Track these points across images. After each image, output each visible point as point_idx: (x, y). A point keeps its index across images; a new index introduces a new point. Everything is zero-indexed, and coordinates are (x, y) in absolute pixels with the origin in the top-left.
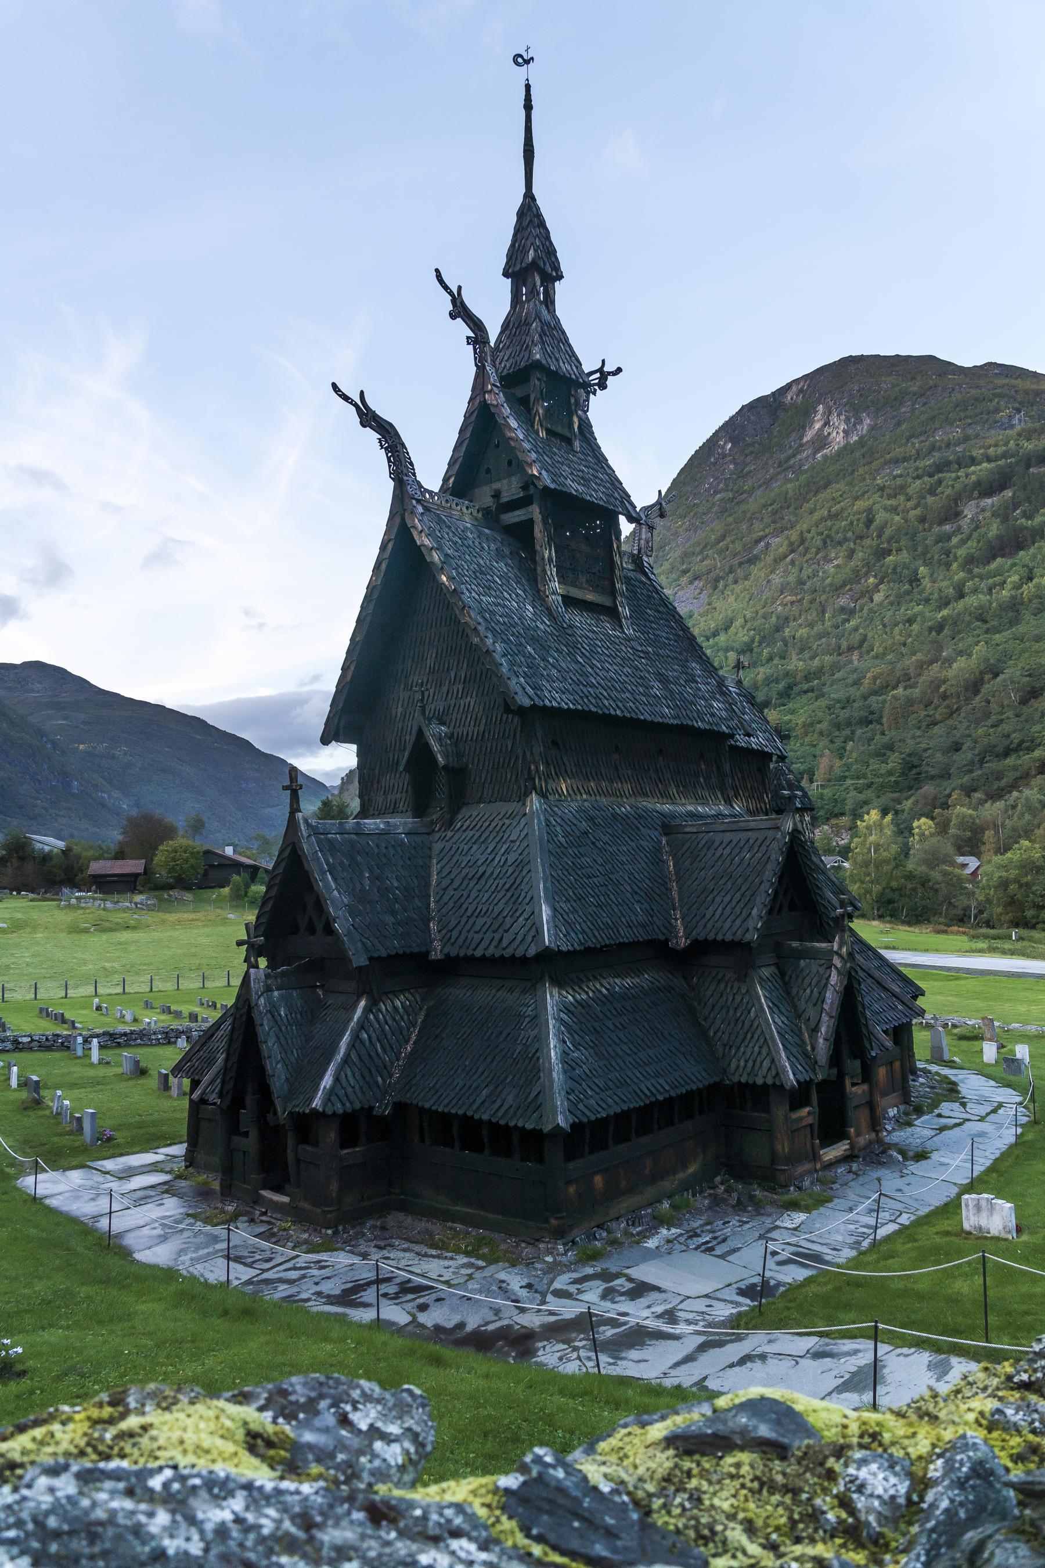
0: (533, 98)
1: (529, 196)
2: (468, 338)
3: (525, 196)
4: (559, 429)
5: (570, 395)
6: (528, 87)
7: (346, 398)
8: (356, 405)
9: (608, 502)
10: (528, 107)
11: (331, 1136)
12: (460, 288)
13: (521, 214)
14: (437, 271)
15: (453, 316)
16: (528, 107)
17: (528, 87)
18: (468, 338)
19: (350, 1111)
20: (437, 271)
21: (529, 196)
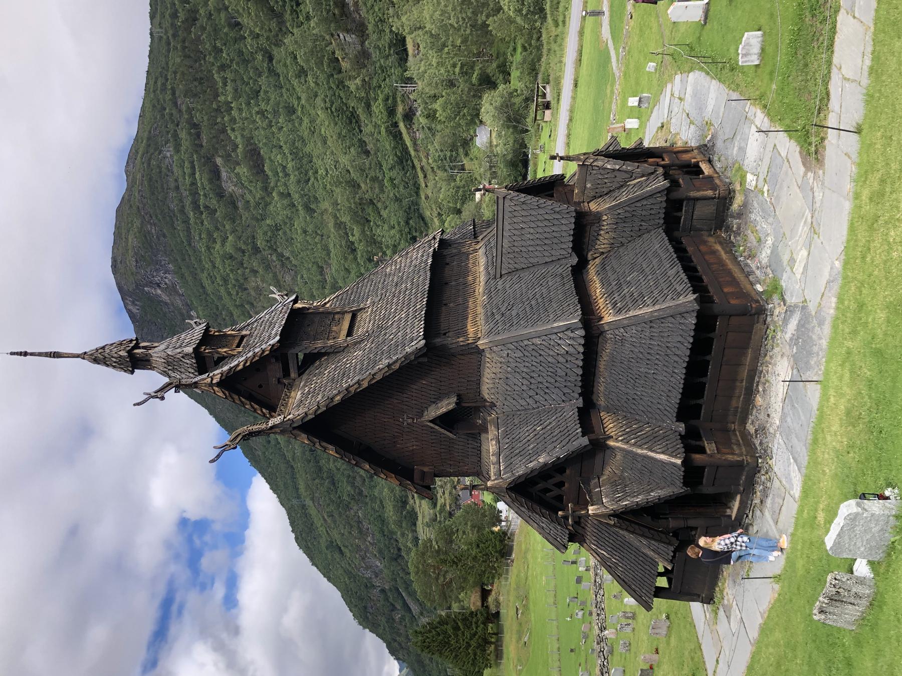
0: (19, 351)
1: (83, 356)
2: (175, 392)
3: (84, 358)
4: (237, 341)
5: (213, 336)
6: (12, 354)
7: (218, 456)
8: (224, 450)
9: (286, 312)
10: (25, 354)
11: (698, 458)
12: (145, 394)
13: (96, 361)
14: (135, 405)
15: (162, 398)
16: (25, 354)
17: (12, 354)
18: (175, 392)
19: (683, 450)
20: (135, 405)
21: (83, 356)
